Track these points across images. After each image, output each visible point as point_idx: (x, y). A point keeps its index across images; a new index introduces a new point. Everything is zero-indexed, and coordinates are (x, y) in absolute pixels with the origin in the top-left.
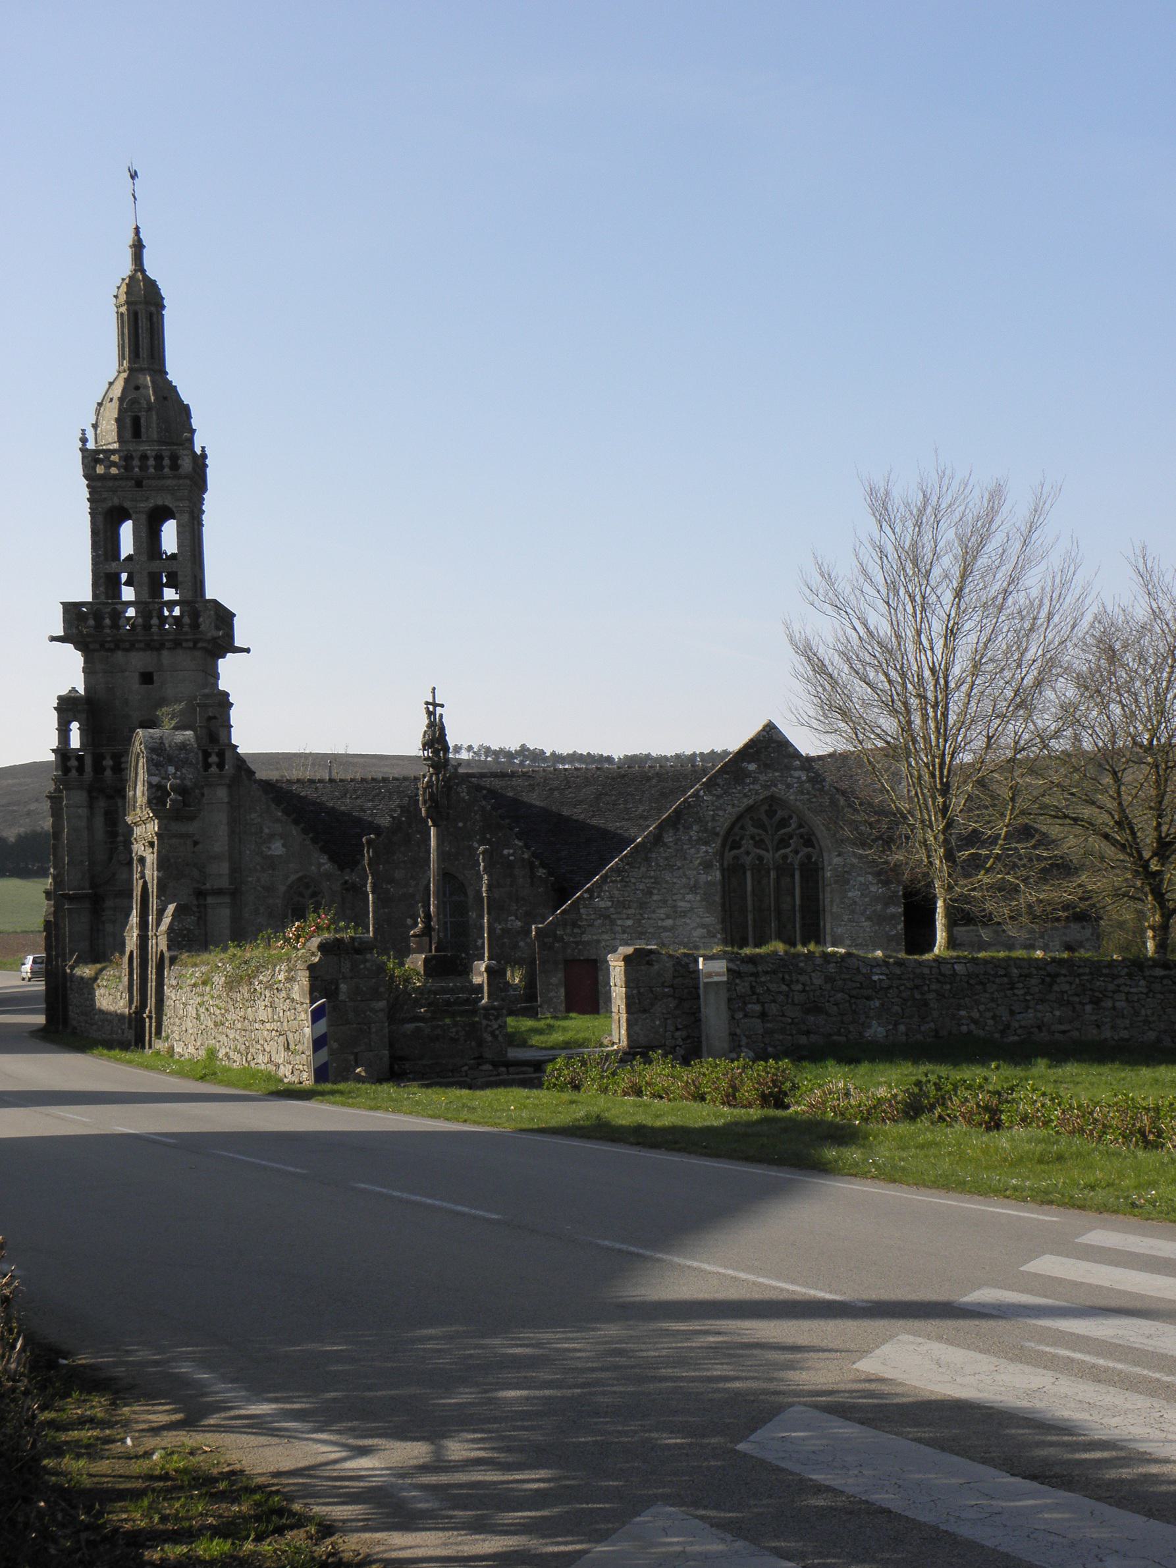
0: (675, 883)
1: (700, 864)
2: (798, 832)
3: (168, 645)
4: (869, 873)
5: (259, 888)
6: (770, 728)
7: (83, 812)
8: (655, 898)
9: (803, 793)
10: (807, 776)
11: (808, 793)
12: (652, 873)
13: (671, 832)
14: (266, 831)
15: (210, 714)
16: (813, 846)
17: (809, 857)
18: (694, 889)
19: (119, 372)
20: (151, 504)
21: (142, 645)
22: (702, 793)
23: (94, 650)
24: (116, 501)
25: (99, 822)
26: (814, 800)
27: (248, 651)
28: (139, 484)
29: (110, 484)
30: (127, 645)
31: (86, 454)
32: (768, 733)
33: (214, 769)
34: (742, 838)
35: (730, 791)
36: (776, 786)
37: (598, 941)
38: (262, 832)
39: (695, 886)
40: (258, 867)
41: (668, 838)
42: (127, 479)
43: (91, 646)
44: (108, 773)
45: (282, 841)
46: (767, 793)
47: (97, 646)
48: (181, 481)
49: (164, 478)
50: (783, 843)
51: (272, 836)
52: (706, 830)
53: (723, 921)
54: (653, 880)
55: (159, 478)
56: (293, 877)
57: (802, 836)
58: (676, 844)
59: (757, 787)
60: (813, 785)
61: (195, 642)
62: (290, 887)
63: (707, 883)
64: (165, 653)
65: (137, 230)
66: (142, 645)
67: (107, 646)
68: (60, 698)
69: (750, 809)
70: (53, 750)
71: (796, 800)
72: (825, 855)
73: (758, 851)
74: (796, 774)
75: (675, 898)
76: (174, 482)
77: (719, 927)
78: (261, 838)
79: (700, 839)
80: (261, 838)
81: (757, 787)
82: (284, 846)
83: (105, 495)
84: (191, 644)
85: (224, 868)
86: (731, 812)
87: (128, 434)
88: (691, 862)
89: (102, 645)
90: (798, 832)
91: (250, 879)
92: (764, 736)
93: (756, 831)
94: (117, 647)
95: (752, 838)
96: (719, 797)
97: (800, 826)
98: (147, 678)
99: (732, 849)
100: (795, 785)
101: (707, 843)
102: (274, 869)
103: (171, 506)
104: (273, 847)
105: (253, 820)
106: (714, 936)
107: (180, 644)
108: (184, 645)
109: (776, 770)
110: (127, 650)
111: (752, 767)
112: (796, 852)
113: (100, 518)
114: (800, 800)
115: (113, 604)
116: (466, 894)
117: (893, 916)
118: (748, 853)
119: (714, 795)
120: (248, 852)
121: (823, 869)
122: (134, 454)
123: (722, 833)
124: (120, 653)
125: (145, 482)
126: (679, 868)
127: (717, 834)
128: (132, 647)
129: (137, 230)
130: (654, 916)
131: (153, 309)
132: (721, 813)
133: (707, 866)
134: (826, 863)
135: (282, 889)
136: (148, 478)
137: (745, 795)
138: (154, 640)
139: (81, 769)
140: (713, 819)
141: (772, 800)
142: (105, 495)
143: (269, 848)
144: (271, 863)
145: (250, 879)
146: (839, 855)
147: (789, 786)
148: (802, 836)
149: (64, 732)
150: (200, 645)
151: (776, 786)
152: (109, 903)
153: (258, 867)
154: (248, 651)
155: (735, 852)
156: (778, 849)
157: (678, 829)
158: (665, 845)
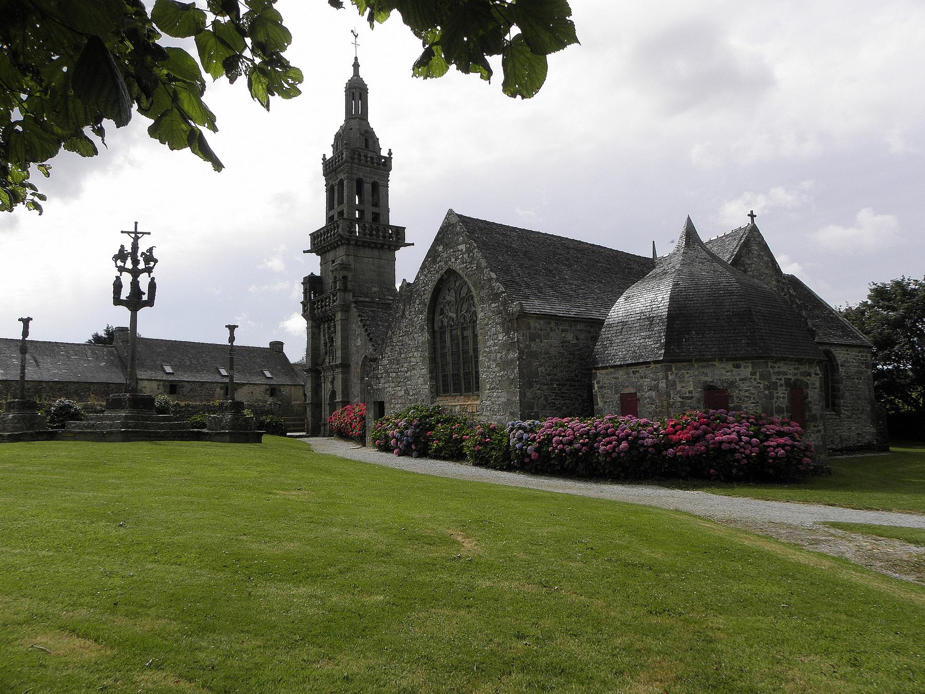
4: (497, 324)
27: (413, 244)
37: (384, 388)
46: (445, 268)
53: (431, 372)
65: (356, 58)
77: (428, 376)
79: (419, 310)
106: (426, 384)
109: (451, 248)
111: (440, 248)
117: (512, 361)
123: (427, 301)
129: (356, 58)
130: (402, 369)
131: (354, 90)
141: (451, 272)
146: (482, 311)
154: (413, 244)
157: (411, 304)
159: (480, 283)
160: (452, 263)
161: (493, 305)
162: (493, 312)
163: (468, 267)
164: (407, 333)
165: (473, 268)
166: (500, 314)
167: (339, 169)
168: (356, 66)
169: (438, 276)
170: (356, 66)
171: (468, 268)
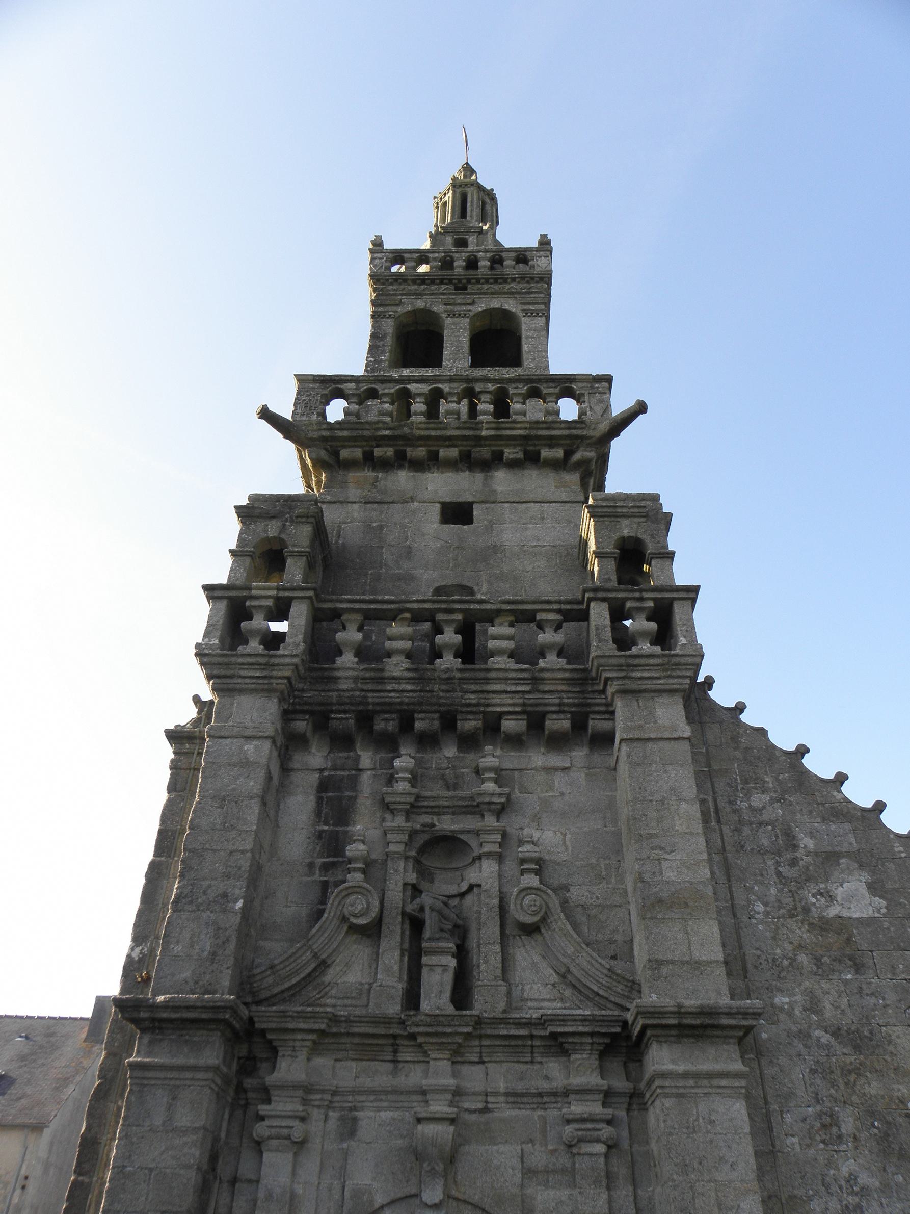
5: (826, 1038)
14: (807, 842)
15: (626, 532)
20: (481, 307)
21: (453, 453)
23: (350, 465)
24: (420, 304)
30: (420, 452)
38: (795, 847)
40: (803, 959)
43: (345, 454)
45: (865, 876)
49: (505, 281)
55: (496, 281)
61: (568, 454)
70: (211, 590)
78: (794, 862)
80: (794, 862)
82: (874, 888)
84: (559, 453)
91: (781, 1000)
94: (401, 460)
102: (858, 968)
103: (514, 310)
104: (839, 893)
105: (761, 810)
108: (545, 453)
110: (418, 466)
113: (389, 327)
115: (402, 380)
120: (760, 908)
128: (432, 462)
136: (478, 281)
138: (478, 440)
145: (781, 1000)
150: (577, 456)
153: (803, 958)
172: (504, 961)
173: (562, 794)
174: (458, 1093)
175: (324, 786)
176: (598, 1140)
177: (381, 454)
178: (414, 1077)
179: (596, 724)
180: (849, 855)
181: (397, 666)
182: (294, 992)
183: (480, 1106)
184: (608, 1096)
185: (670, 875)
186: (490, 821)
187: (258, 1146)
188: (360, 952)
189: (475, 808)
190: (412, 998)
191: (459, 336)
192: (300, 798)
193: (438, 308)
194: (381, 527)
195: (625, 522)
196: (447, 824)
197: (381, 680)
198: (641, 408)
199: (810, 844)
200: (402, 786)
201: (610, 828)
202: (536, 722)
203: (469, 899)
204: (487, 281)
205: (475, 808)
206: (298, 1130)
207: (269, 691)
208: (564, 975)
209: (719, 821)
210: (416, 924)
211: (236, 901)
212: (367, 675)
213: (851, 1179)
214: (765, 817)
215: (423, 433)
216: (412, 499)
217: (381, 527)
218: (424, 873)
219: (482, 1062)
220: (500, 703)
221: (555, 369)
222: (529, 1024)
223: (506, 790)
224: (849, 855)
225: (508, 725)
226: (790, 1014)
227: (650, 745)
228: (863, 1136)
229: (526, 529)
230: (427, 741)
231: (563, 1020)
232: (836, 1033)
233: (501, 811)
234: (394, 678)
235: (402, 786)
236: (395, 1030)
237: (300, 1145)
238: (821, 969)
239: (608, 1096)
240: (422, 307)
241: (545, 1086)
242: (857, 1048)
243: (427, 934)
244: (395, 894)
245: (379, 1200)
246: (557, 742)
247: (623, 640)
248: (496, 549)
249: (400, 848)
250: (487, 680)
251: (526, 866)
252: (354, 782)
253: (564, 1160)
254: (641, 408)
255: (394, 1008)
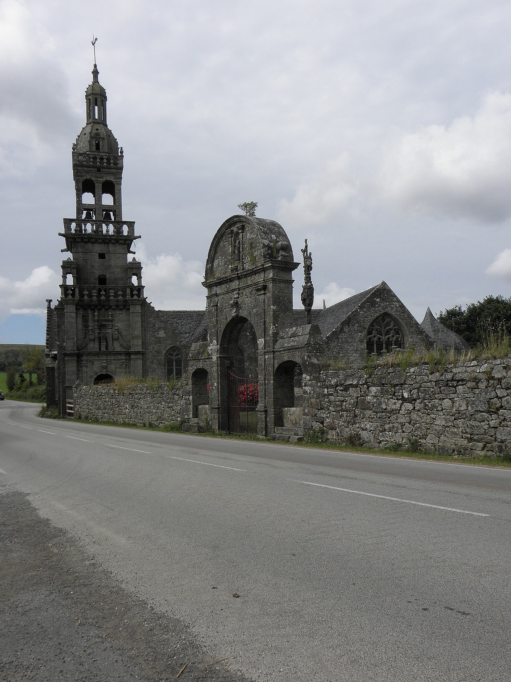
0: (349, 349)
1: (358, 340)
2: (393, 328)
3: (113, 241)
6: (384, 283)
7: (73, 315)
8: (341, 355)
9: (397, 312)
10: (399, 305)
11: (399, 312)
12: (340, 344)
13: (347, 327)
14: (157, 326)
16: (399, 334)
17: (397, 339)
18: (356, 351)
19: (87, 124)
20: (104, 179)
21: (101, 241)
22: (359, 310)
23: (78, 242)
24: (88, 177)
25: (80, 320)
26: (401, 314)
28: (99, 170)
29: (86, 169)
30: (94, 240)
31: (75, 154)
32: (383, 286)
33: (135, 297)
34: (372, 330)
35: (370, 310)
36: (387, 308)
39: (356, 350)
41: (346, 329)
42: (94, 167)
43: (77, 240)
44: (86, 297)
45: (164, 331)
46: (383, 312)
47: (80, 240)
48: (118, 171)
50: (388, 333)
51: (159, 328)
52: (361, 326)
54: (340, 347)
56: (169, 347)
57: (395, 330)
58: (349, 332)
59: (380, 308)
60: (401, 308)
62: (167, 351)
63: (362, 349)
64: (110, 245)
66: (101, 241)
67: (84, 240)
68: (64, 262)
69: (377, 318)
71: (395, 314)
72: (406, 338)
73: (379, 336)
74: (395, 303)
75: (349, 355)
76: (115, 171)
79: (358, 330)
81: (380, 308)
83: (83, 174)
84: (123, 242)
85: (140, 342)
86: (371, 319)
87: (94, 149)
88: (355, 340)
89: (82, 240)
90: (393, 328)
92: (382, 287)
93: (378, 327)
94: (89, 241)
95: (376, 330)
96: (365, 312)
97: (394, 326)
98: (102, 256)
99: (368, 335)
100: (394, 308)
101: (361, 332)
103: (113, 181)
107: (118, 241)
109: (387, 302)
110: (92, 243)
111: (378, 300)
112: (393, 336)
114: (396, 315)
116: (243, 355)
118: (375, 337)
119: (364, 311)
120: (149, 335)
121: (404, 343)
122: (97, 157)
124: (90, 244)
125: (101, 170)
126: (350, 343)
127: (365, 328)
132: (366, 319)
133: (361, 341)
134: (405, 341)
135: (164, 352)
136: (103, 168)
137: (376, 312)
139: (73, 295)
140: (364, 322)
141: (386, 314)
142: (83, 174)
143: (158, 334)
144: (159, 341)
146: (411, 338)
147: (392, 309)
148: (395, 330)
149: (64, 277)
150: (127, 242)
151: (387, 308)
152: (84, 358)
153: (153, 342)
155: (369, 336)
156: (386, 335)
158: (344, 332)
159: (410, 324)
160: (389, 310)
161: (419, 336)
162: (420, 339)
163: (401, 314)
164: (347, 342)
165: (404, 316)
166: (424, 341)
167: (104, 170)
168: (95, 73)
169: (377, 315)
170: (95, 73)
171: (401, 315)
172: (113, 343)
173: (121, 318)
174: (107, 359)
175: (83, 316)
176: (125, 364)
177: (85, 241)
178: (101, 358)
179: (127, 307)
180: (162, 328)
181: (95, 299)
182: (83, 348)
183: (110, 361)
184: (126, 360)
185: (136, 333)
186: (110, 323)
187: (82, 367)
188: (92, 343)
189: (108, 321)
190: (100, 349)
191: (99, 191)
192: (79, 319)
193: (93, 179)
194: (87, 259)
195: (134, 270)
196: (103, 323)
197: (92, 301)
198: (140, 237)
199: (157, 326)
200: (96, 318)
201: (129, 323)
202: (117, 306)
203: (107, 334)
204: (106, 168)
205: (108, 321)
206: (87, 365)
207: (74, 304)
208: (121, 345)
209: (145, 323)
210: (100, 338)
211: (75, 338)
212: (90, 300)
213: (154, 367)
214: (152, 322)
215: (94, 237)
216: (92, 252)
217: (87, 259)
218: (100, 329)
219: (110, 356)
220: (111, 305)
221: (124, 219)
222: (116, 352)
223: (113, 318)
224: (162, 328)
225: (113, 307)
226: (150, 349)
227: (135, 313)
228: (156, 363)
229: (116, 261)
230: (100, 309)
231: (121, 351)
232: (156, 351)
233: (112, 321)
234: (94, 301)
235: (96, 318)
236: (99, 353)
237: (87, 366)
238: (155, 344)
239: (126, 360)
240: (89, 178)
241: (118, 358)
242: (158, 353)
243: (101, 340)
244: (97, 334)
245: (98, 372)
246: (121, 310)
247: (132, 295)
248: (110, 266)
249: (96, 327)
250: (110, 301)
251: (116, 330)
252: (88, 316)
253: (121, 367)
254: (140, 237)
255: (98, 350)
